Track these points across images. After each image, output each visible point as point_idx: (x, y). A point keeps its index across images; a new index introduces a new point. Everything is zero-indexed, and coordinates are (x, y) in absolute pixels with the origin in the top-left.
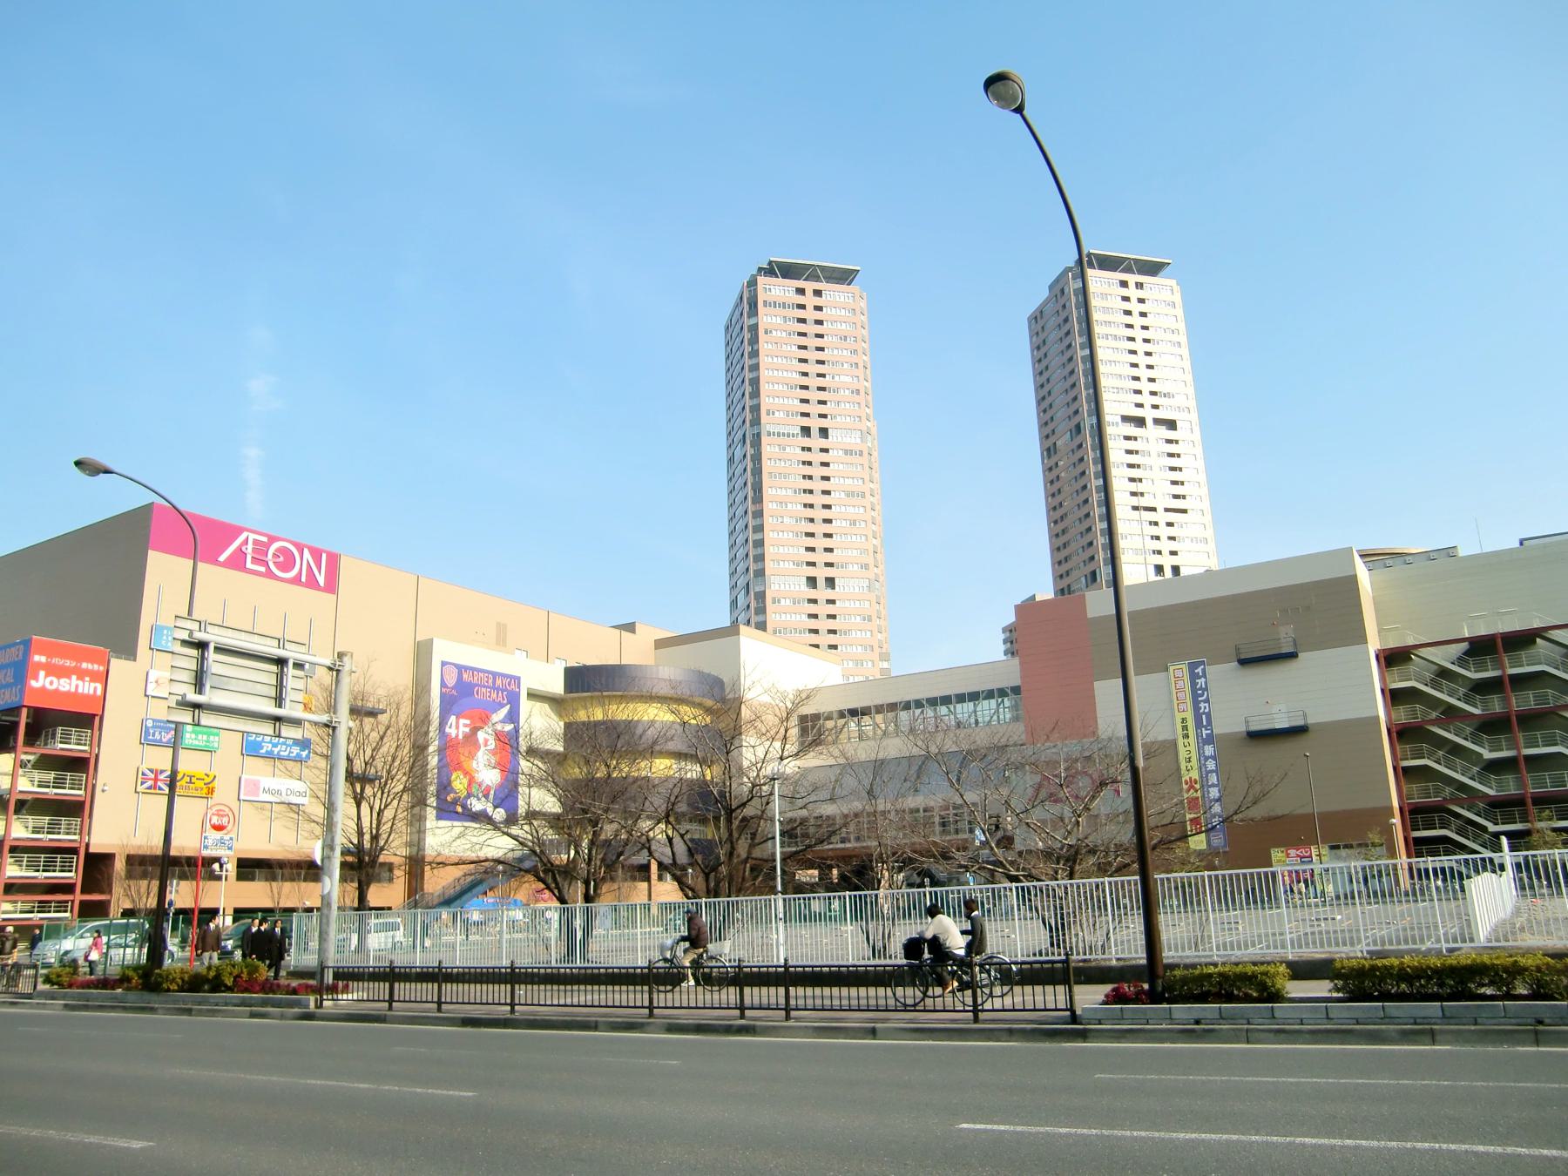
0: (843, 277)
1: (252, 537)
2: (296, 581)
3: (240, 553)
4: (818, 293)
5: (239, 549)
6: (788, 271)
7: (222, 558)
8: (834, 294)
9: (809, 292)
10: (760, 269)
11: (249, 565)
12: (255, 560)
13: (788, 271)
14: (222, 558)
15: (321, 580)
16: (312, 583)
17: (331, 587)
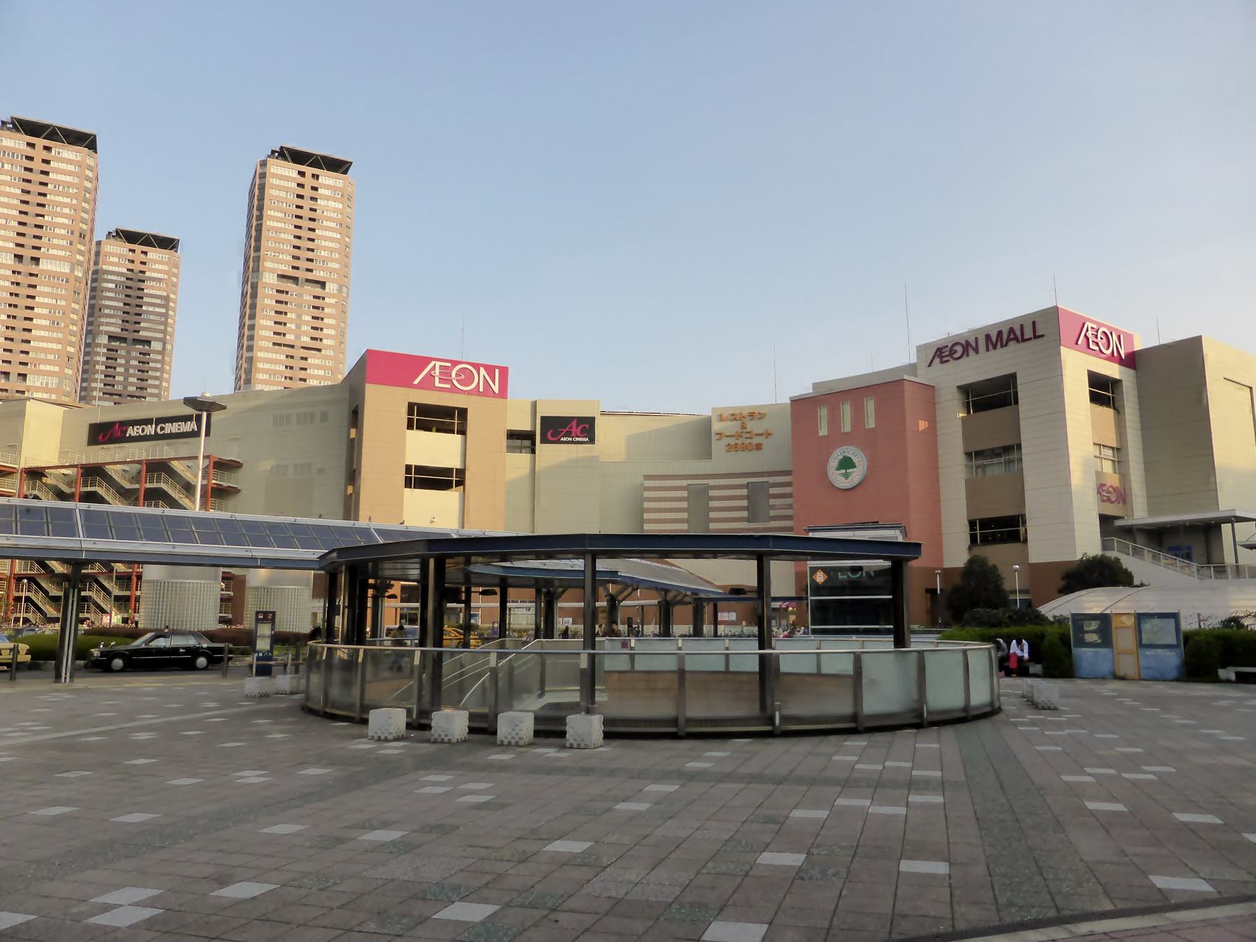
0: (338, 166)
1: (438, 364)
2: (476, 392)
3: (430, 376)
4: (315, 177)
5: (429, 373)
6: (298, 157)
7: (416, 382)
8: (328, 179)
9: (309, 175)
10: (273, 152)
11: (437, 384)
12: (441, 381)
13: (298, 157)
14: (416, 382)
15: (496, 389)
16: (488, 392)
17: (503, 393)
